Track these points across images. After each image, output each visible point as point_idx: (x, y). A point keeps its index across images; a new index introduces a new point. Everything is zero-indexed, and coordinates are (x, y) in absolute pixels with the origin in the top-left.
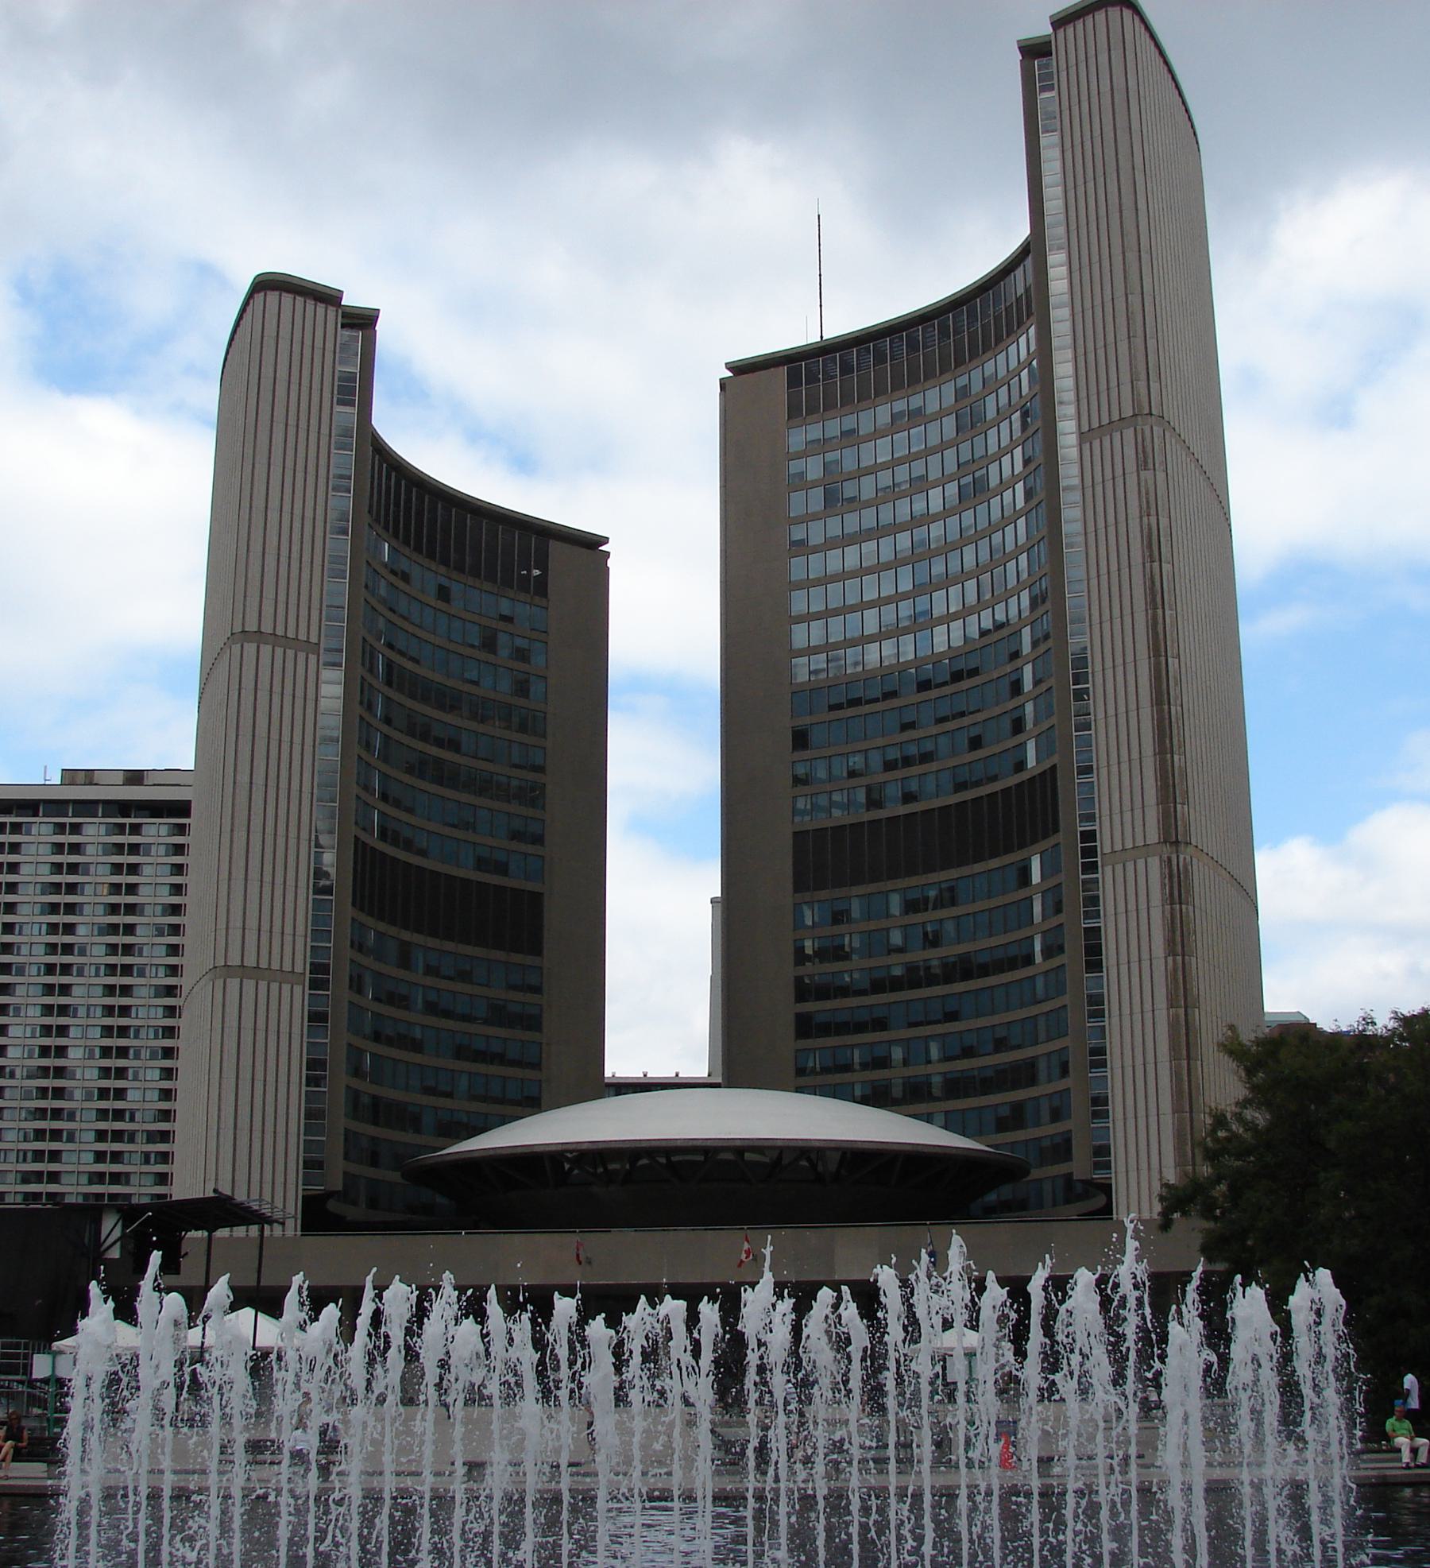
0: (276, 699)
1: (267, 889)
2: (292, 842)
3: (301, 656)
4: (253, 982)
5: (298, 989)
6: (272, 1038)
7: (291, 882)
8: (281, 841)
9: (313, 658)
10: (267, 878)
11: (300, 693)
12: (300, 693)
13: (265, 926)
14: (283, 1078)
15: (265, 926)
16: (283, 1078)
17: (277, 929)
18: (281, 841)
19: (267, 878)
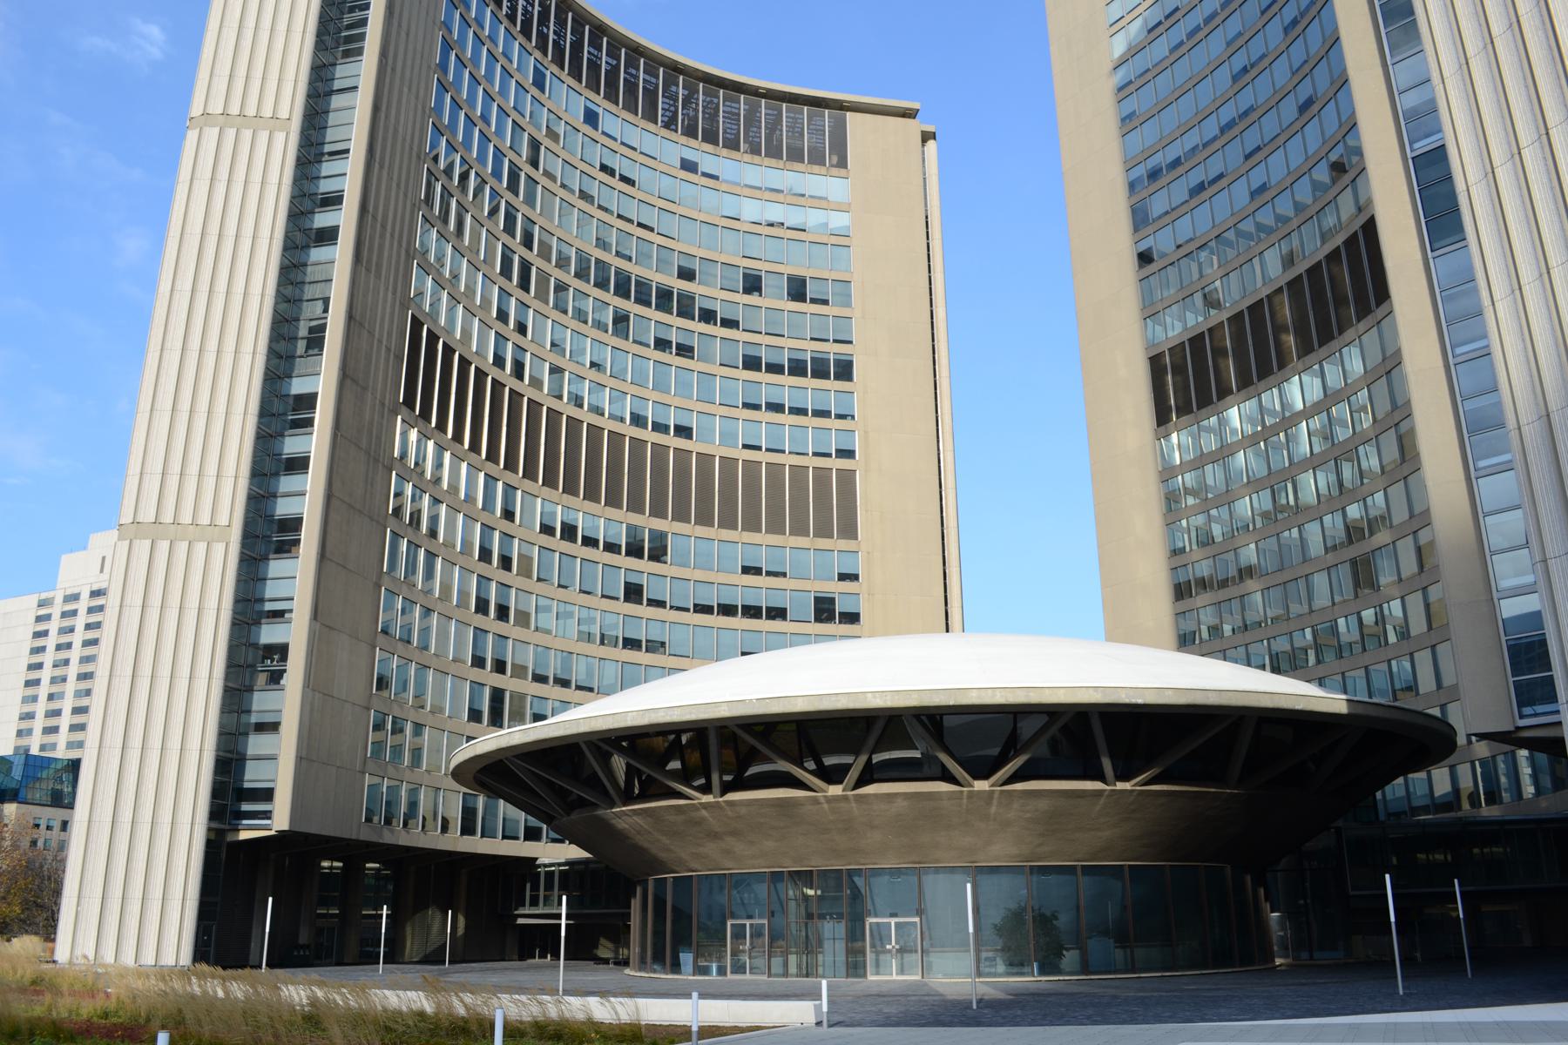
0: (221, 189)
1: (183, 417)
2: (228, 360)
3: (263, 137)
4: (148, 543)
5: (219, 548)
6: (173, 616)
7: (220, 408)
8: (210, 359)
9: (280, 137)
10: (185, 405)
11: (257, 176)
12: (257, 176)
13: (176, 467)
14: (184, 670)
15: (176, 467)
16: (184, 670)
17: (193, 469)
18: (210, 359)
19: (185, 405)
